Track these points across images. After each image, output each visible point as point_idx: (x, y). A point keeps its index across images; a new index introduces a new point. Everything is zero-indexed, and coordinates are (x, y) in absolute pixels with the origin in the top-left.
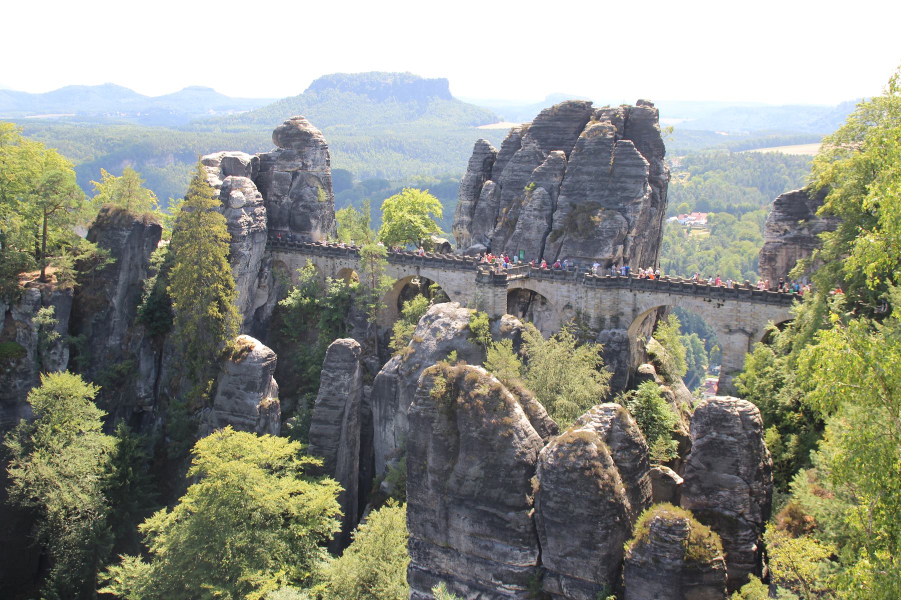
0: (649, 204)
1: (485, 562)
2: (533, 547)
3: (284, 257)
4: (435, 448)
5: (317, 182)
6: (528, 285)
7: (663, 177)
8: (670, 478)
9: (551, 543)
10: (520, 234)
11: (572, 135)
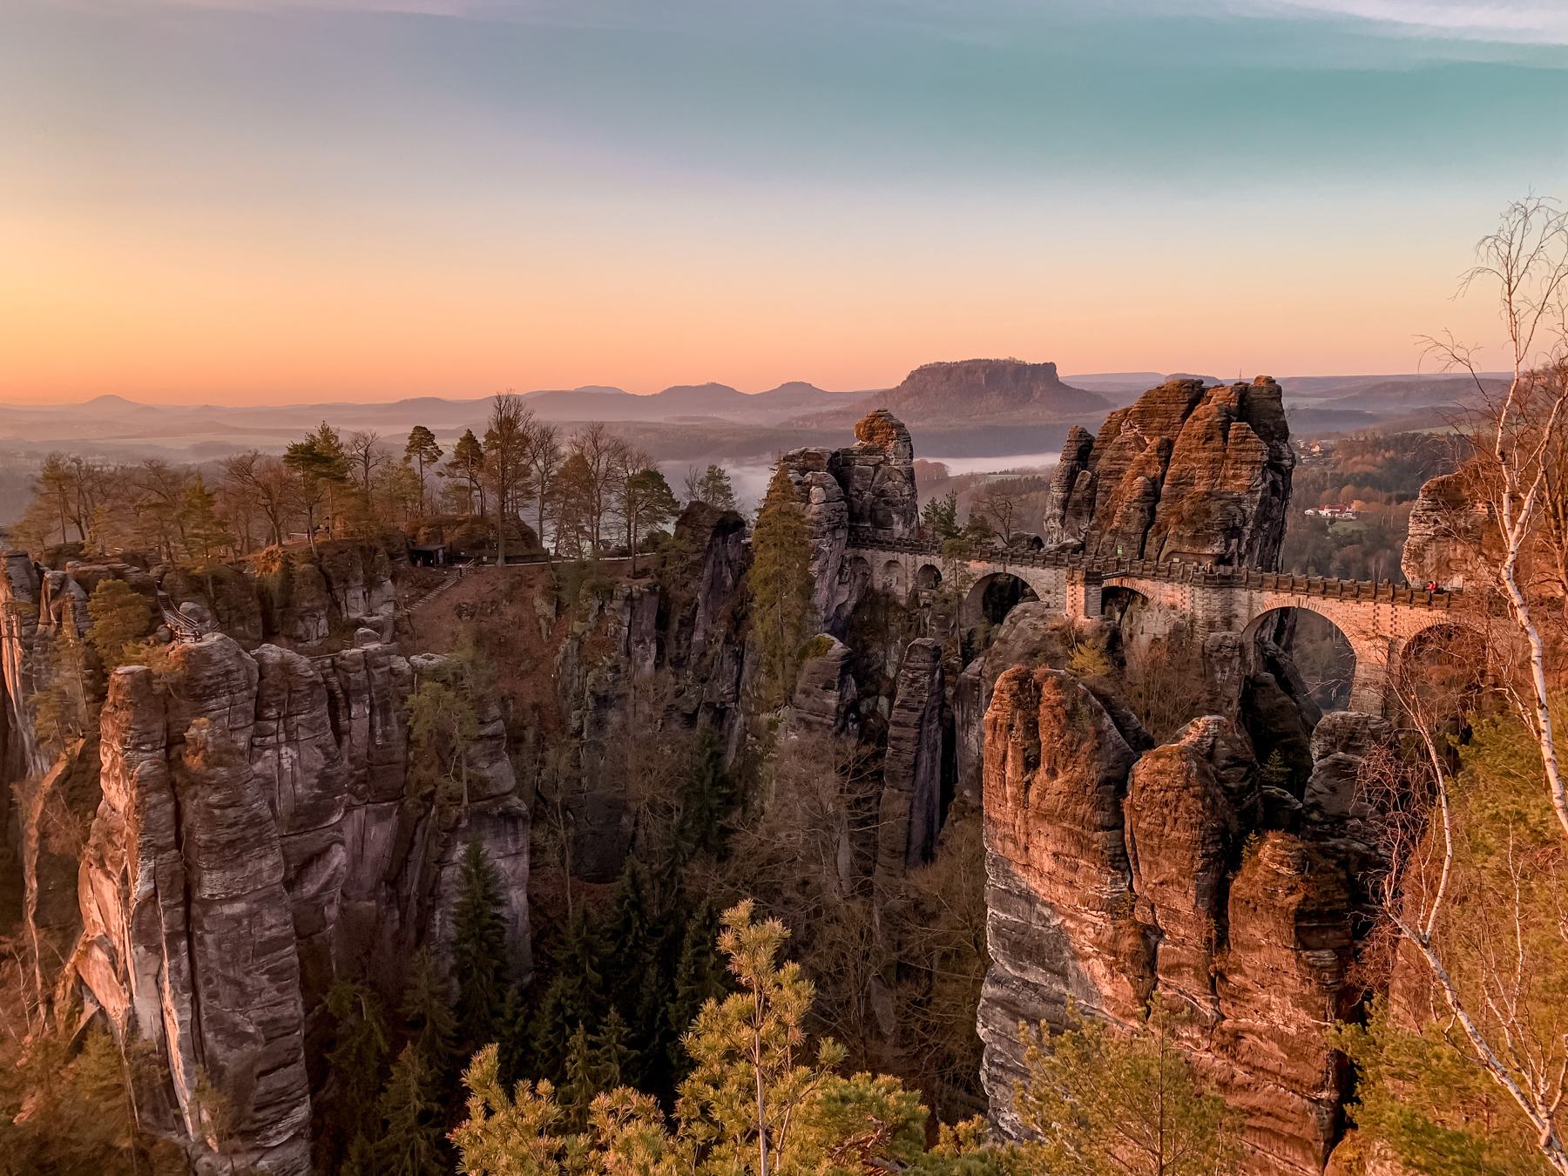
0: (1269, 493)
1: (1071, 884)
2: (1123, 871)
3: (867, 554)
4: (1014, 758)
5: (899, 477)
6: (1126, 584)
7: (1287, 462)
8: (1287, 802)
9: (1143, 869)
10: (1117, 530)
11: (1178, 419)
